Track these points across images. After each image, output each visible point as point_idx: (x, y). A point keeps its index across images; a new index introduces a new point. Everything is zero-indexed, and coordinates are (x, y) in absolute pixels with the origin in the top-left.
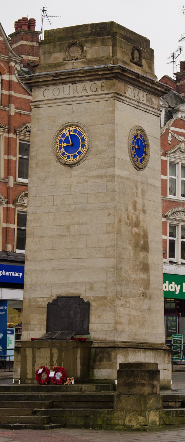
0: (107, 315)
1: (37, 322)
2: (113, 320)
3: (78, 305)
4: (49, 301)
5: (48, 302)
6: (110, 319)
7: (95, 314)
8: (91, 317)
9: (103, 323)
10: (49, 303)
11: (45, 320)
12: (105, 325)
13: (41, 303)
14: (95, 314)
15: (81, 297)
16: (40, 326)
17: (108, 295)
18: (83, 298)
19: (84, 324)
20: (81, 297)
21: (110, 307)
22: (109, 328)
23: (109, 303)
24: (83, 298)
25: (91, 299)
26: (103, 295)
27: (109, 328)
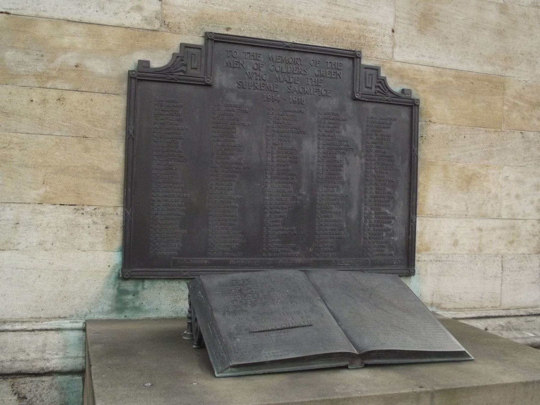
0: (506, 178)
1: (42, 191)
2: (532, 202)
3: (350, 105)
4: (142, 56)
5: (140, 62)
6: (517, 196)
7: (445, 167)
8: (421, 179)
9: (484, 216)
10: (143, 65)
11: (108, 178)
12: (494, 229)
13: (73, 62)
14: (445, 167)
15: (364, 62)
16: (67, 213)
17: (509, 73)
18: (377, 69)
19: (389, 219)
20: (364, 62)
21: (517, 134)
22: (511, 242)
23: (514, 115)
24: (377, 69)
25: (423, 82)
26: (488, 69)
27: (511, 242)
